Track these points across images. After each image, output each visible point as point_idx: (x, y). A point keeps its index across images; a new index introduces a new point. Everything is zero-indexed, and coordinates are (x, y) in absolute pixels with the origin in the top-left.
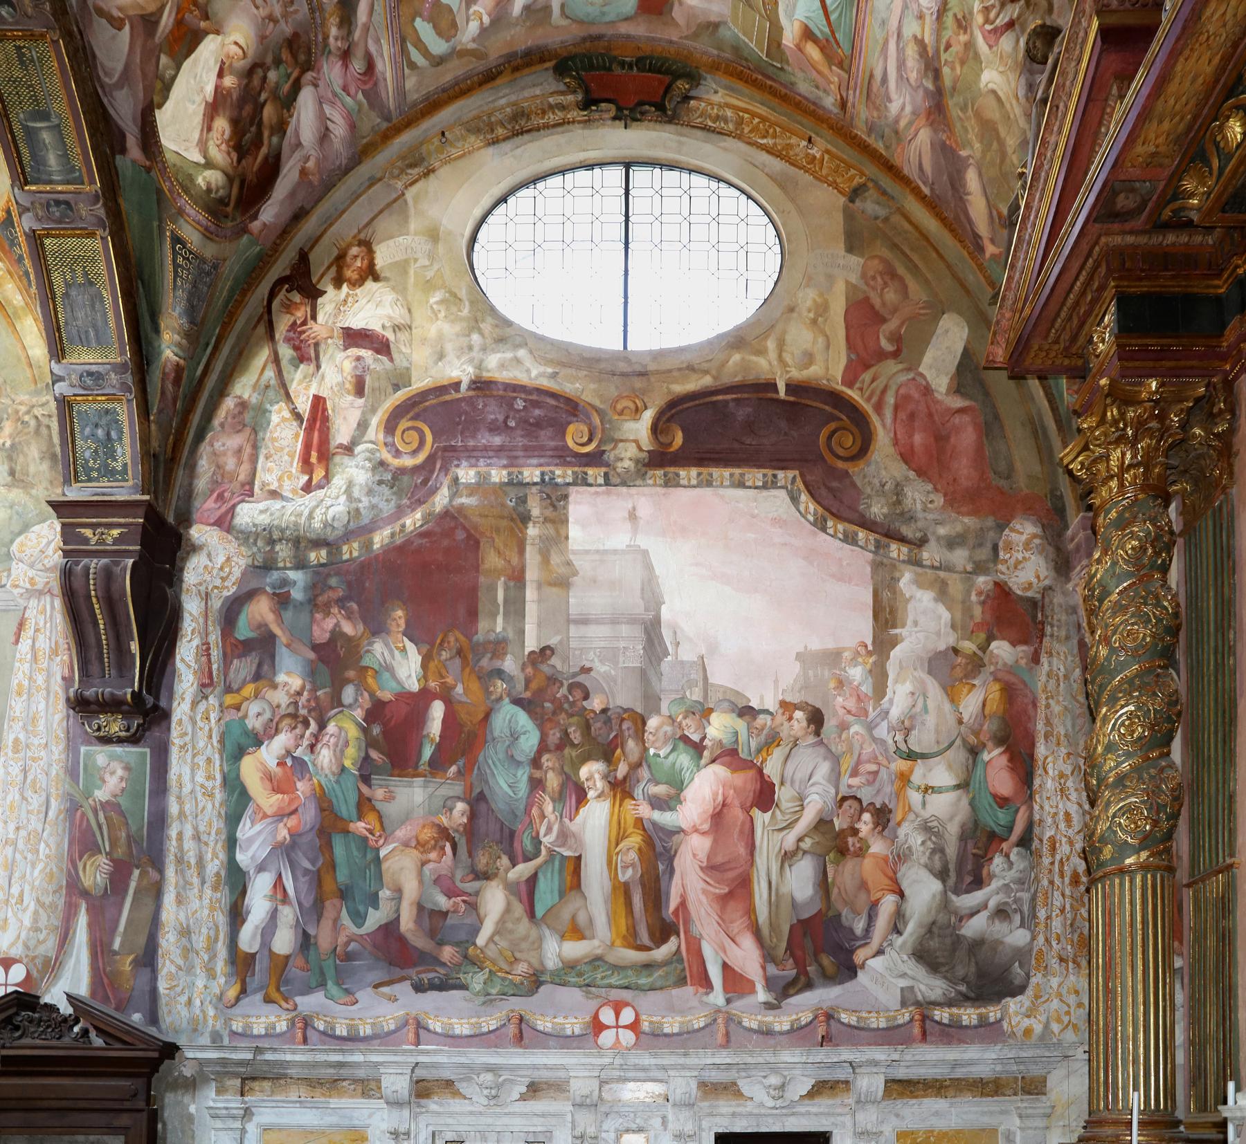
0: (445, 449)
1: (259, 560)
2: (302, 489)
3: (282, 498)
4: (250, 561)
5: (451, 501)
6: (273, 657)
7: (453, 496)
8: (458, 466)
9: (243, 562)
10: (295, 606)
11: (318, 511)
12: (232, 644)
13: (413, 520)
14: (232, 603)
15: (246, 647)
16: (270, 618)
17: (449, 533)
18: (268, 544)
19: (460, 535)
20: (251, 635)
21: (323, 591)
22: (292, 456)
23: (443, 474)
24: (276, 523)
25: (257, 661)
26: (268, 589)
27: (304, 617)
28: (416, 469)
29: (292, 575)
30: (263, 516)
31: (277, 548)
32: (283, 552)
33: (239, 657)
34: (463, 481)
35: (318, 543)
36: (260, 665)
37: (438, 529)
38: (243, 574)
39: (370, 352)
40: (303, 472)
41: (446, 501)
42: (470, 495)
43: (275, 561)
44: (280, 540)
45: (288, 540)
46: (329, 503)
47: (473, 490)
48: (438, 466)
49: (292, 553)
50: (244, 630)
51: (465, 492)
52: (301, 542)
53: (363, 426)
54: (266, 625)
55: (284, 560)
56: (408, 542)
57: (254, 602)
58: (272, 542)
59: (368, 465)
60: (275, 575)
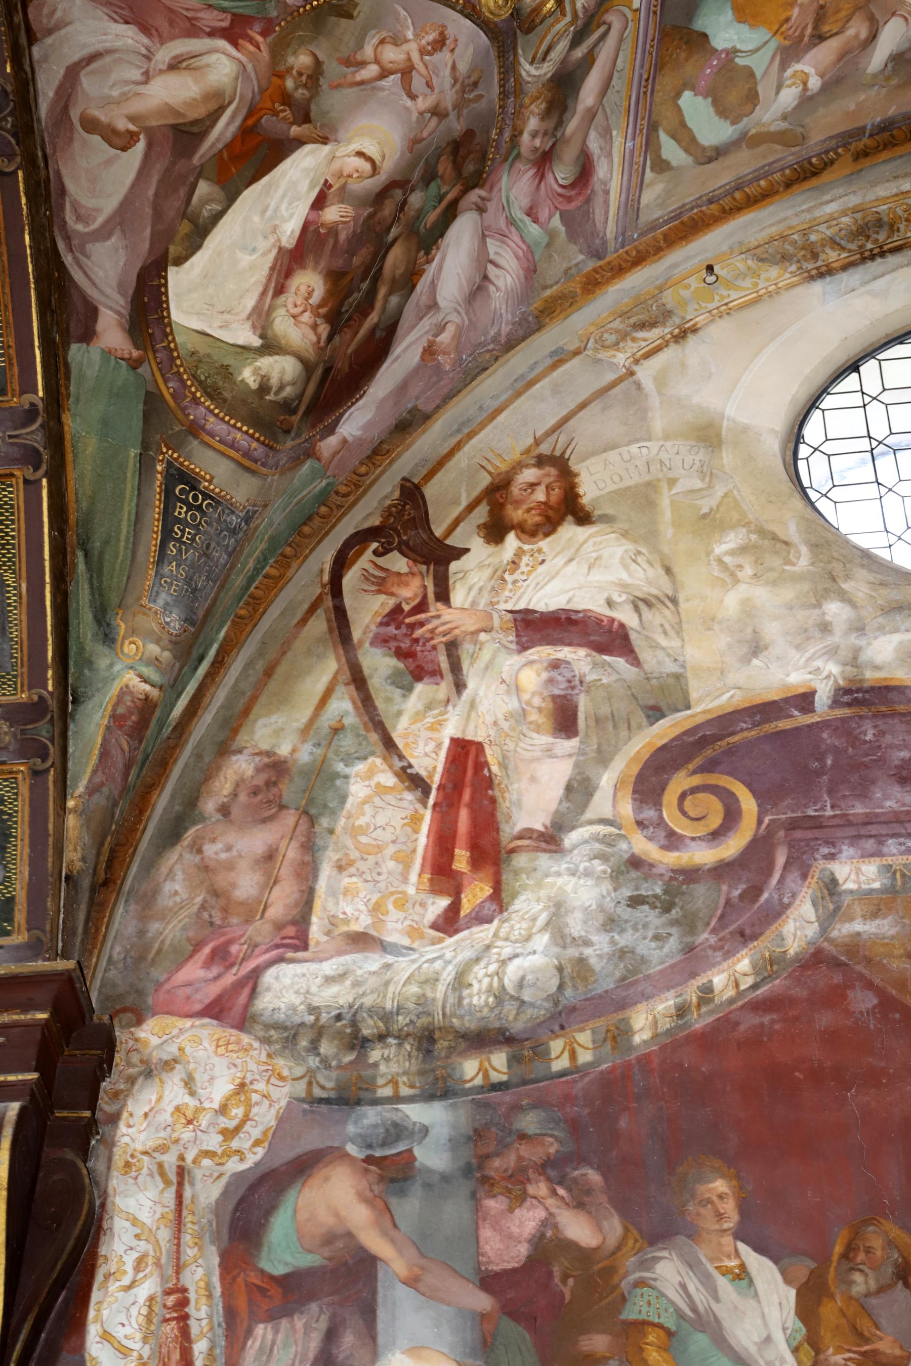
0: (793, 825)
1: (328, 1082)
2: (434, 926)
3: (383, 947)
4: (300, 1089)
5: (824, 929)
6: (369, 1312)
7: (826, 921)
8: (832, 857)
9: (282, 1094)
10: (428, 1186)
11: (479, 971)
12: (252, 1288)
13: (731, 975)
14: (253, 1188)
15: (291, 1292)
16: (360, 1219)
17: (835, 997)
18: (352, 1047)
19: (863, 1001)
20: (307, 1260)
21: (503, 1147)
22: (405, 861)
23: (794, 875)
24: (368, 1001)
25: (323, 1324)
26: (352, 1149)
27: (454, 1211)
28: (721, 870)
29: (417, 1113)
30: (334, 989)
31: (375, 1055)
32: (390, 1064)
33: (271, 1317)
34: (851, 885)
35: (481, 1039)
36: (331, 1336)
37: (800, 992)
38: (282, 1120)
39: (582, 652)
40: (436, 890)
41: (812, 931)
42: (875, 914)
43: (370, 1085)
44: (382, 1037)
45: (401, 1037)
46: (507, 951)
47: (877, 904)
48: (781, 859)
49: (414, 1065)
50: (284, 1248)
51: (858, 910)
52: (435, 1041)
53: (579, 790)
54: (349, 1235)
55: (394, 1082)
56: (726, 1023)
57: (315, 1181)
58: (358, 1043)
59: (599, 866)
60: (371, 1116)
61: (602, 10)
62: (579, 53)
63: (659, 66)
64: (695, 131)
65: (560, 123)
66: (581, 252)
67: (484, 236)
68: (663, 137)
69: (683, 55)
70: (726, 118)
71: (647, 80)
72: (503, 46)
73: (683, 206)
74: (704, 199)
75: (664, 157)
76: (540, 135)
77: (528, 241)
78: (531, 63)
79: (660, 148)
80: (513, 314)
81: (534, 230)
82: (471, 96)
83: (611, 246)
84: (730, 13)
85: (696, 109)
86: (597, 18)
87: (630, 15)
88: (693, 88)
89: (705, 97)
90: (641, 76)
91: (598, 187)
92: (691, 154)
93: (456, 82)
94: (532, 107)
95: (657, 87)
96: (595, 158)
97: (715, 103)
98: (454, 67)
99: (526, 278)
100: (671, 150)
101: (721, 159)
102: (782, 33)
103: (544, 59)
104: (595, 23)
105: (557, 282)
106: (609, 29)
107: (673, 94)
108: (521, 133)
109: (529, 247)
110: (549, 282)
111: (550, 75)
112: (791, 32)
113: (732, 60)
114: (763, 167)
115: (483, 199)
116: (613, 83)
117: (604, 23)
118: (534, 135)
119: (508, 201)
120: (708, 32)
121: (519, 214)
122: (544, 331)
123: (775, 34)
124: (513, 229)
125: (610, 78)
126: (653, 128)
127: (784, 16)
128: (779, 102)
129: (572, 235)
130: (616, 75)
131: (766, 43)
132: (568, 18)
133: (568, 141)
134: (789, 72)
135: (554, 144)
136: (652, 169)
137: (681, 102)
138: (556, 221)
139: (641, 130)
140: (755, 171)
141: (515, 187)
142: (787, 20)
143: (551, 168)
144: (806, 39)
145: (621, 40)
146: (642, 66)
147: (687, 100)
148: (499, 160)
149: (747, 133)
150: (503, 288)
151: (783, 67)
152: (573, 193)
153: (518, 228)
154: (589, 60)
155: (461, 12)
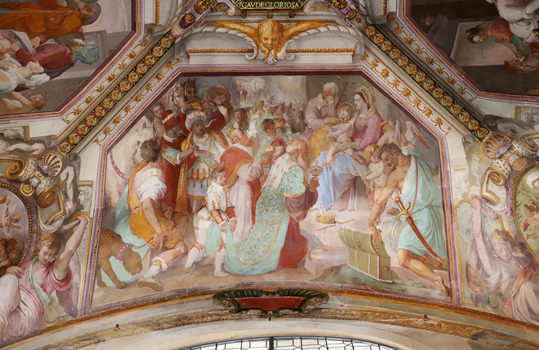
61: (77, 214)
62: (66, 227)
63: (101, 243)
64: (116, 273)
65: (57, 253)
66: (65, 311)
67: (19, 289)
68: (103, 272)
69: (111, 241)
70: (129, 272)
71: (96, 247)
72: (30, 209)
73: (111, 304)
74: (121, 304)
75: (103, 281)
76: (48, 255)
77: (40, 298)
78: (45, 224)
79: (101, 276)
80: (31, 329)
81: (43, 295)
82: (15, 225)
83: (79, 313)
84: (130, 230)
85: (116, 264)
86: (75, 216)
87: (89, 219)
88: (115, 256)
89: (120, 261)
90: (93, 245)
91: (73, 285)
92: (114, 283)
93: (7, 215)
94: (45, 242)
95: (100, 251)
96: (73, 272)
97: (124, 264)
98: (7, 210)
99: (39, 315)
100: (105, 278)
101: (127, 288)
102: (151, 243)
103: (51, 224)
104: (74, 218)
105: (54, 322)
106: (80, 222)
107: (107, 256)
108: (39, 251)
109: (41, 301)
110: (49, 321)
111: (53, 232)
112: (154, 243)
113: (131, 248)
114: (145, 296)
115: (20, 272)
116: (81, 244)
117: (78, 219)
118: (45, 254)
119: (32, 278)
120: (121, 235)
121: (37, 286)
122: (42, 336)
123: (148, 242)
124: (34, 291)
125: (80, 242)
126: (98, 267)
127: (151, 236)
128: (150, 272)
129: (61, 302)
130: (82, 241)
131: (144, 245)
132: (62, 212)
133: (61, 261)
134: (154, 259)
135: (54, 261)
136: (98, 284)
137: (110, 260)
138: (54, 294)
139: (93, 267)
140: (142, 297)
141: (35, 273)
142: (153, 238)
143: (52, 270)
144: (160, 248)
145: (85, 228)
146: (94, 241)
147: (112, 259)
148: (28, 258)
149: (138, 280)
150: (27, 316)
151: (152, 257)
152: (62, 284)
153: (36, 291)
154: (70, 232)
155: (13, 192)
